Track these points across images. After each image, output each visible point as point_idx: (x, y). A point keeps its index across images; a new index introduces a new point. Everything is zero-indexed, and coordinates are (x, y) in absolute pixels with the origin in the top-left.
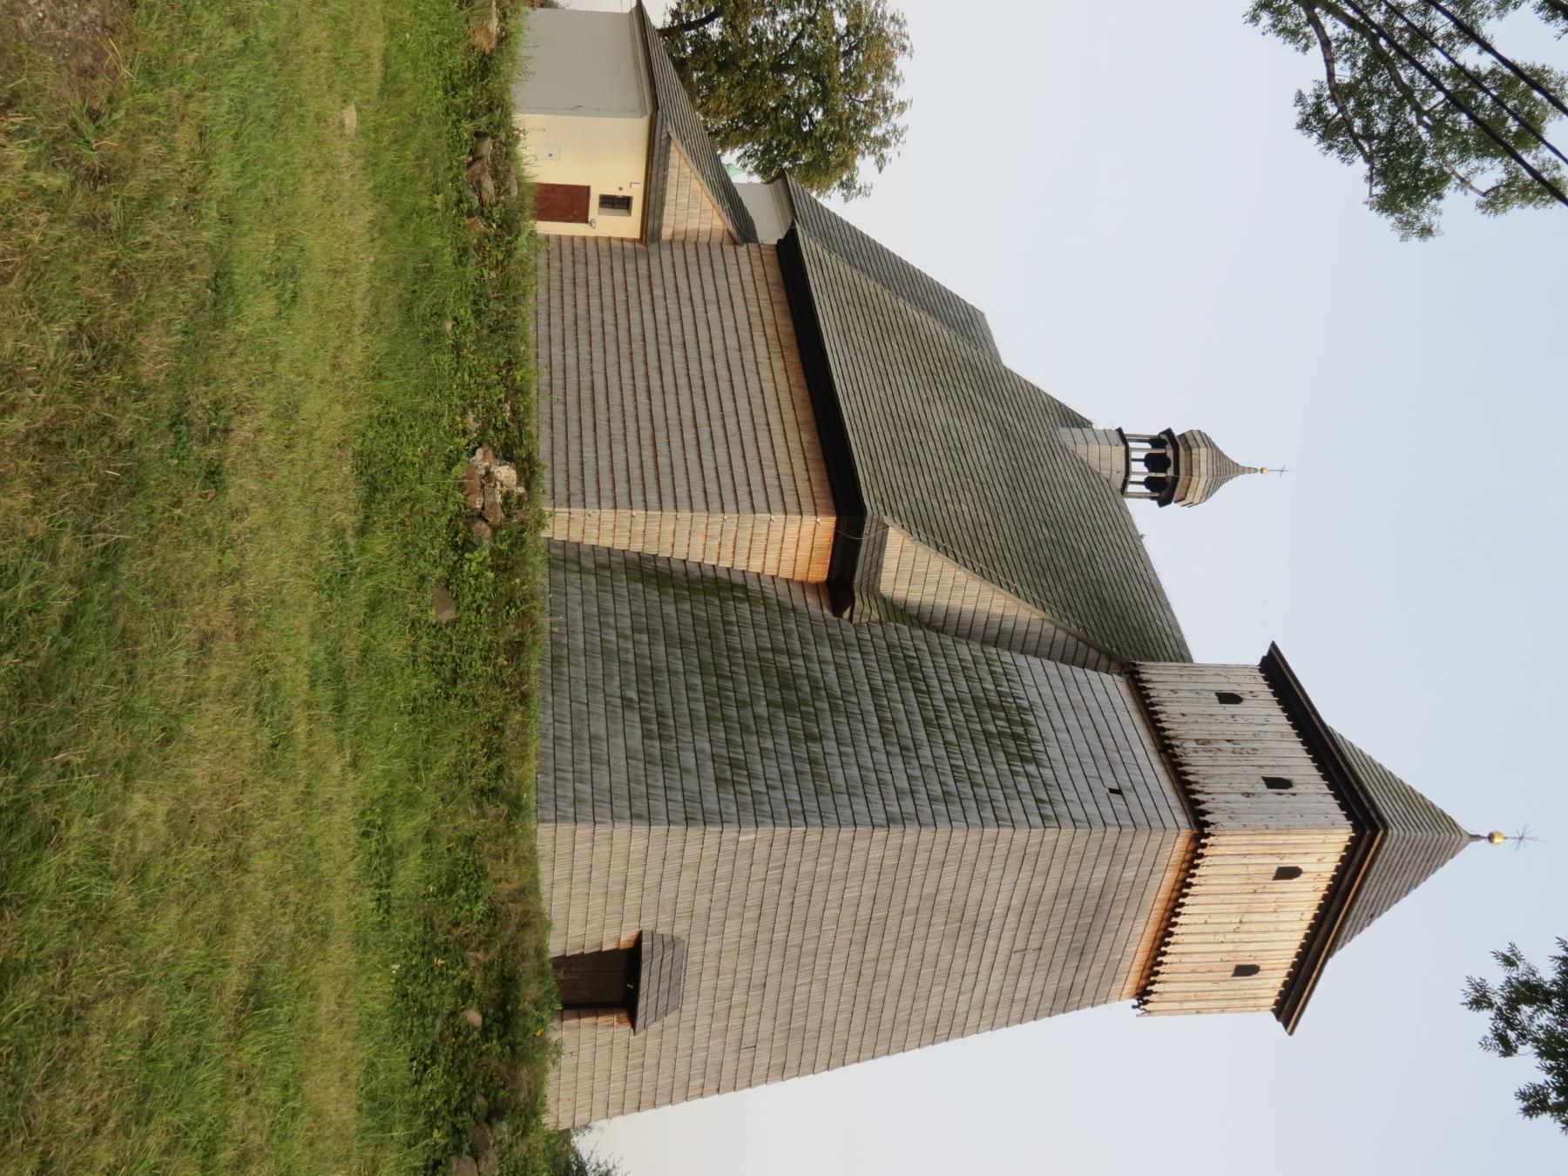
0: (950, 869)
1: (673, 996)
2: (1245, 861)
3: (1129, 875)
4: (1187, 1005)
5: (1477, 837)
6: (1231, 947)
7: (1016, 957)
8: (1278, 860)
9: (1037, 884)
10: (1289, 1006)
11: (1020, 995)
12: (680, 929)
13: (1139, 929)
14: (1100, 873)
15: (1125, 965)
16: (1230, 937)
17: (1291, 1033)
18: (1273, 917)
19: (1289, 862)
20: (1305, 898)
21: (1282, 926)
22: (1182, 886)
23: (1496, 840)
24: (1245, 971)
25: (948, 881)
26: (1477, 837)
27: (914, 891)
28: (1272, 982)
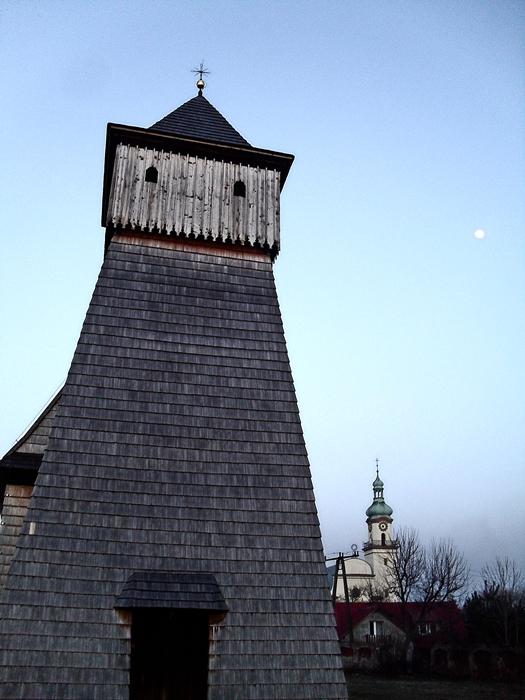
0: (106, 382)
1: (207, 579)
2: (136, 201)
3: (144, 268)
4: (270, 219)
5: (200, 93)
6: (216, 202)
7: (210, 332)
8: (139, 185)
9: (139, 325)
10: (281, 163)
11: (252, 327)
12: (121, 576)
13: (199, 257)
14: (139, 286)
15: (234, 263)
16: (206, 202)
17: (293, 157)
18: (191, 181)
19: (141, 175)
20: (170, 164)
21: (200, 173)
22: (159, 235)
23: (201, 83)
24: (240, 189)
25: (117, 383)
26: (200, 93)
27: (123, 406)
28: (249, 173)
